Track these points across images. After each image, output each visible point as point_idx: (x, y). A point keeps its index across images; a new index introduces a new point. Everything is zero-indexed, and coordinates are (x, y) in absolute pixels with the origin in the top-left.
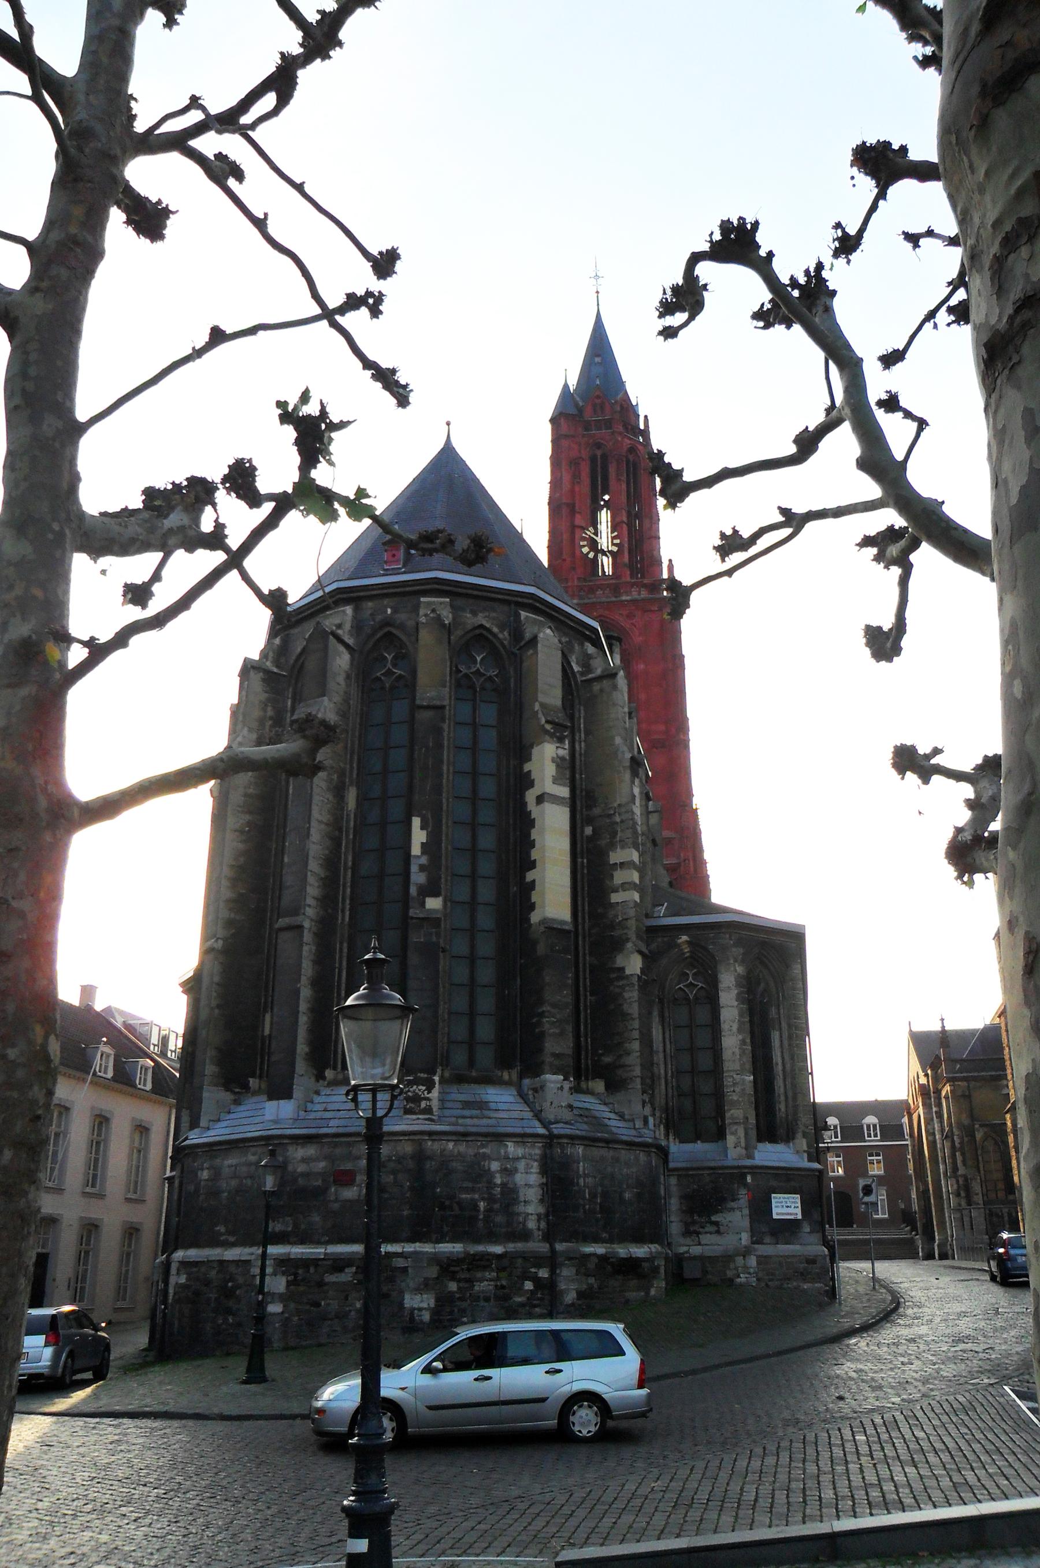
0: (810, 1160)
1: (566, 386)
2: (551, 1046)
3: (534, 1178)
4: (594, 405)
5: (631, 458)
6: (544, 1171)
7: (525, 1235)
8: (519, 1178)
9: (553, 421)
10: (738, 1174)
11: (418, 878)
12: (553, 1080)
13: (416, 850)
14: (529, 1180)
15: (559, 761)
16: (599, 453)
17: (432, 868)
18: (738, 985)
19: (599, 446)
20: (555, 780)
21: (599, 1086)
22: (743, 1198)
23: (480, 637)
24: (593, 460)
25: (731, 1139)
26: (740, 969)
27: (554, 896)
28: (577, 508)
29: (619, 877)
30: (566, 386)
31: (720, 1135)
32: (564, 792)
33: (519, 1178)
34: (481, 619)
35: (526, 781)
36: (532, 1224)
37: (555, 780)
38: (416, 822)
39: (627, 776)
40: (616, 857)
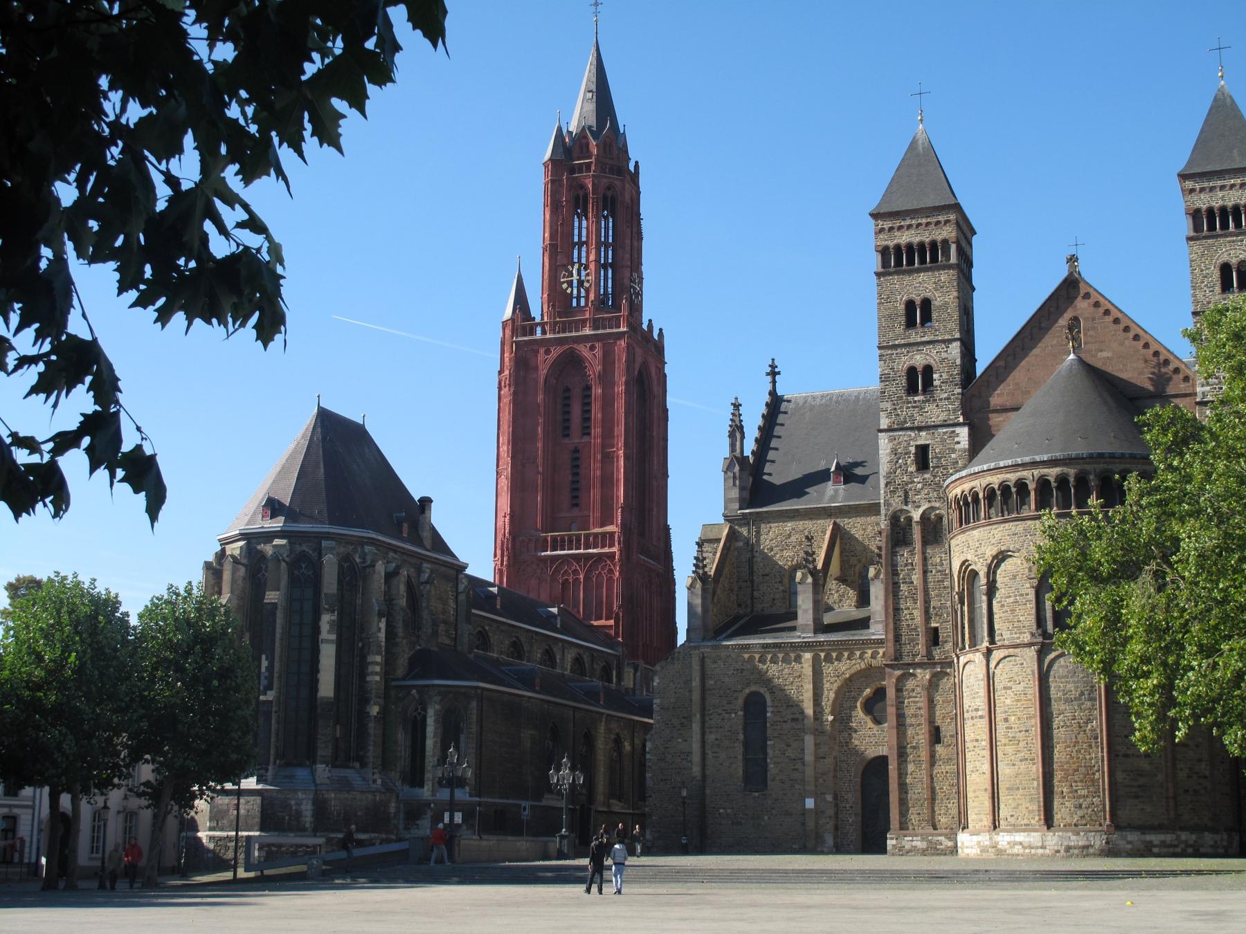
0: (471, 795)
2: (320, 753)
3: (310, 807)
5: (609, 194)
6: (314, 804)
7: (305, 830)
8: (303, 807)
10: (428, 804)
11: (264, 682)
12: (320, 767)
13: (263, 670)
14: (307, 809)
15: (331, 623)
16: (581, 193)
17: (270, 678)
18: (437, 713)
20: (329, 632)
21: (357, 765)
22: (429, 814)
23: (303, 556)
25: (426, 788)
26: (437, 707)
27: (326, 686)
29: (371, 669)
31: (422, 786)
32: (334, 637)
33: (303, 807)
34: (304, 548)
35: (316, 630)
36: (308, 825)
37: (329, 632)
38: (264, 657)
39: (376, 619)
40: (370, 659)
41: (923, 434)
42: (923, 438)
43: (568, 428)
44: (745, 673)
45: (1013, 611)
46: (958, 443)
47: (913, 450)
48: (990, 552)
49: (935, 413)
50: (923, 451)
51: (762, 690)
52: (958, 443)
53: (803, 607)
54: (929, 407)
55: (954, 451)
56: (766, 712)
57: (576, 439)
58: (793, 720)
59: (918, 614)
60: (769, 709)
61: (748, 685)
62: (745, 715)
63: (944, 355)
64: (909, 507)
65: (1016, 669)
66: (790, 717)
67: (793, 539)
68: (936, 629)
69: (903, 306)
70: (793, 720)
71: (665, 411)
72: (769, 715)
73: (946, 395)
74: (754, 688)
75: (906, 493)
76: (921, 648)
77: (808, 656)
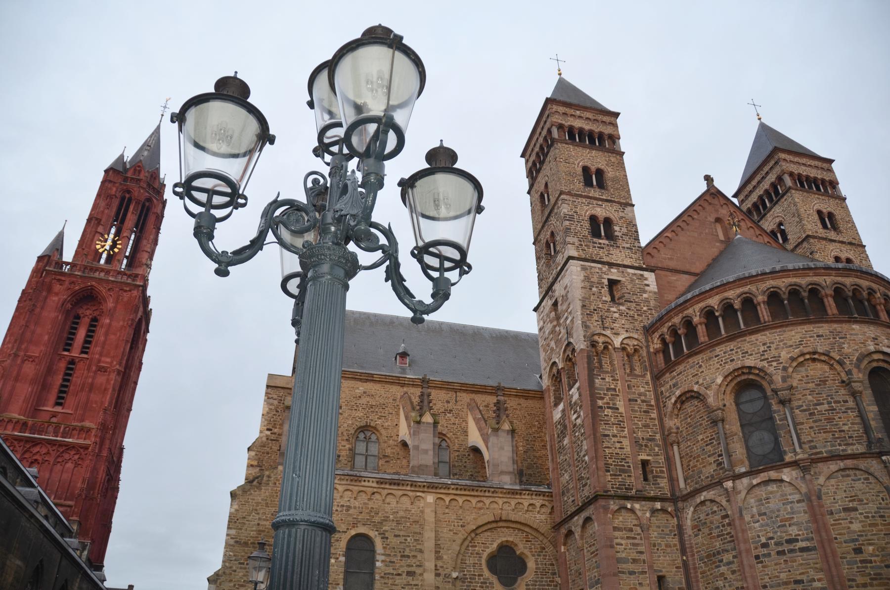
1: (122, 156)
4: (135, 170)
5: (147, 204)
9: (106, 171)
19: (129, 192)
24: (123, 199)
28: (102, 223)
30: (122, 156)
41: (614, 270)
42: (614, 274)
43: (70, 345)
44: (351, 511)
45: (830, 420)
46: (648, 285)
47: (606, 282)
48: (784, 355)
49: (618, 256)
50: (612, 283)
51: (372, 534)
52: (648, 285)
53: (423, 446)
54: (614, 251)
55: (645, 292)
56: (373, 561)
57: (75, 353)
58: (409, 574)
59: (626, 442)
60: (379, 558)
61: (355, 525)
62: (347, 563)
63: (621, 214)
64: (608, 332)
65: (859, 485)
66: (406, 569)
67: (364, 401)
68: (645, 463)
69: (581, 169)
70: (409, 574)
71: (141, 364)
72: (378, 564)
73: (628, 245)
74: (362, 530)
75: (603, 319)
76: (635, 480)
77: (430, 498)
